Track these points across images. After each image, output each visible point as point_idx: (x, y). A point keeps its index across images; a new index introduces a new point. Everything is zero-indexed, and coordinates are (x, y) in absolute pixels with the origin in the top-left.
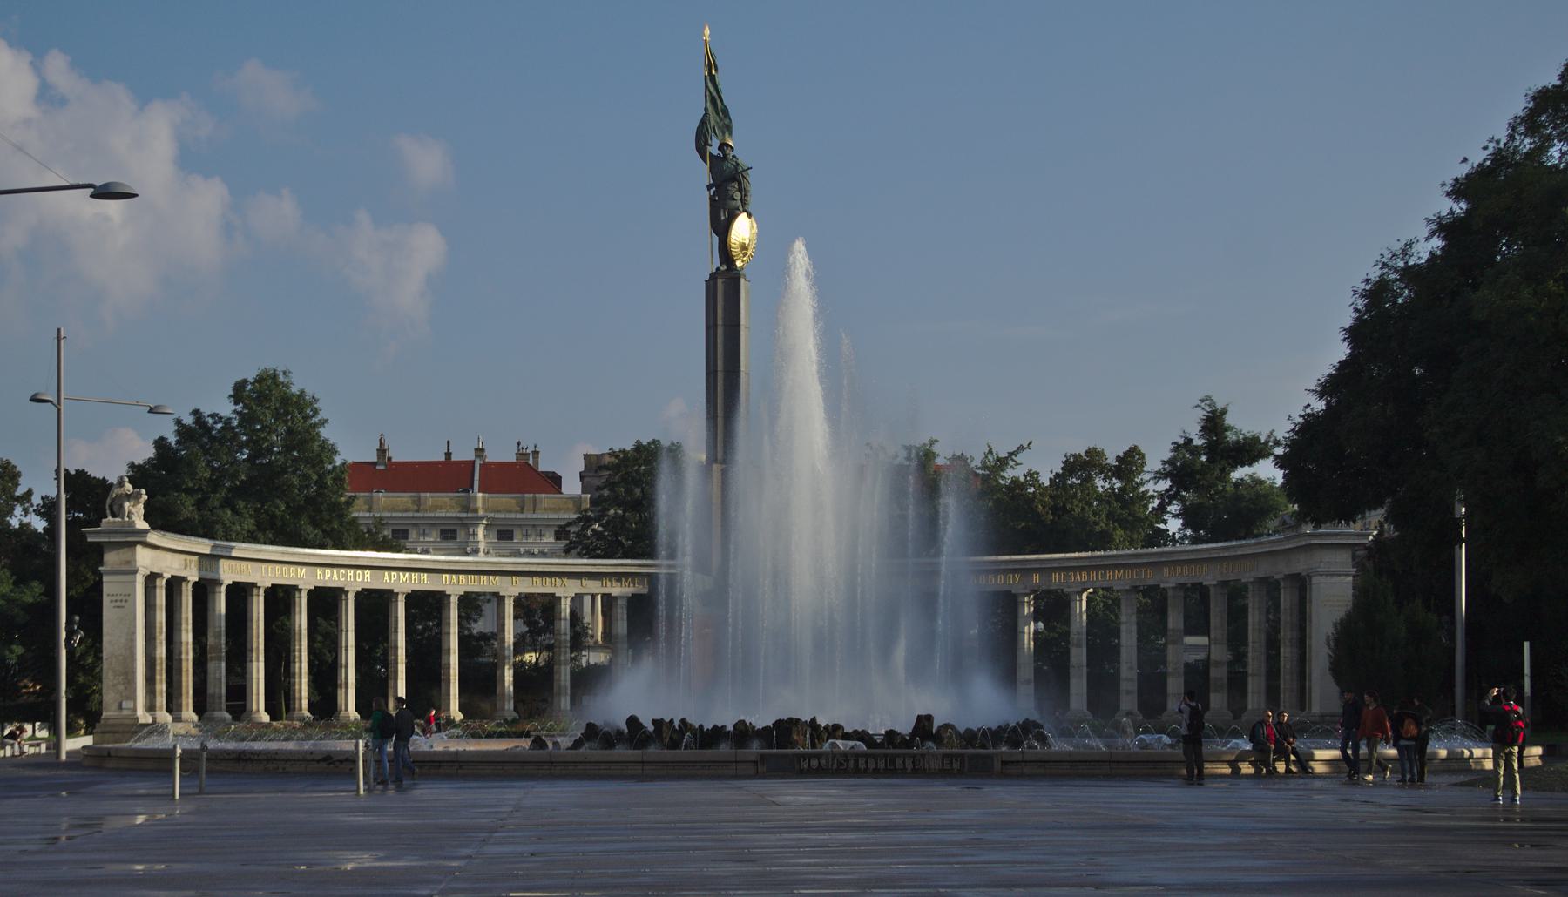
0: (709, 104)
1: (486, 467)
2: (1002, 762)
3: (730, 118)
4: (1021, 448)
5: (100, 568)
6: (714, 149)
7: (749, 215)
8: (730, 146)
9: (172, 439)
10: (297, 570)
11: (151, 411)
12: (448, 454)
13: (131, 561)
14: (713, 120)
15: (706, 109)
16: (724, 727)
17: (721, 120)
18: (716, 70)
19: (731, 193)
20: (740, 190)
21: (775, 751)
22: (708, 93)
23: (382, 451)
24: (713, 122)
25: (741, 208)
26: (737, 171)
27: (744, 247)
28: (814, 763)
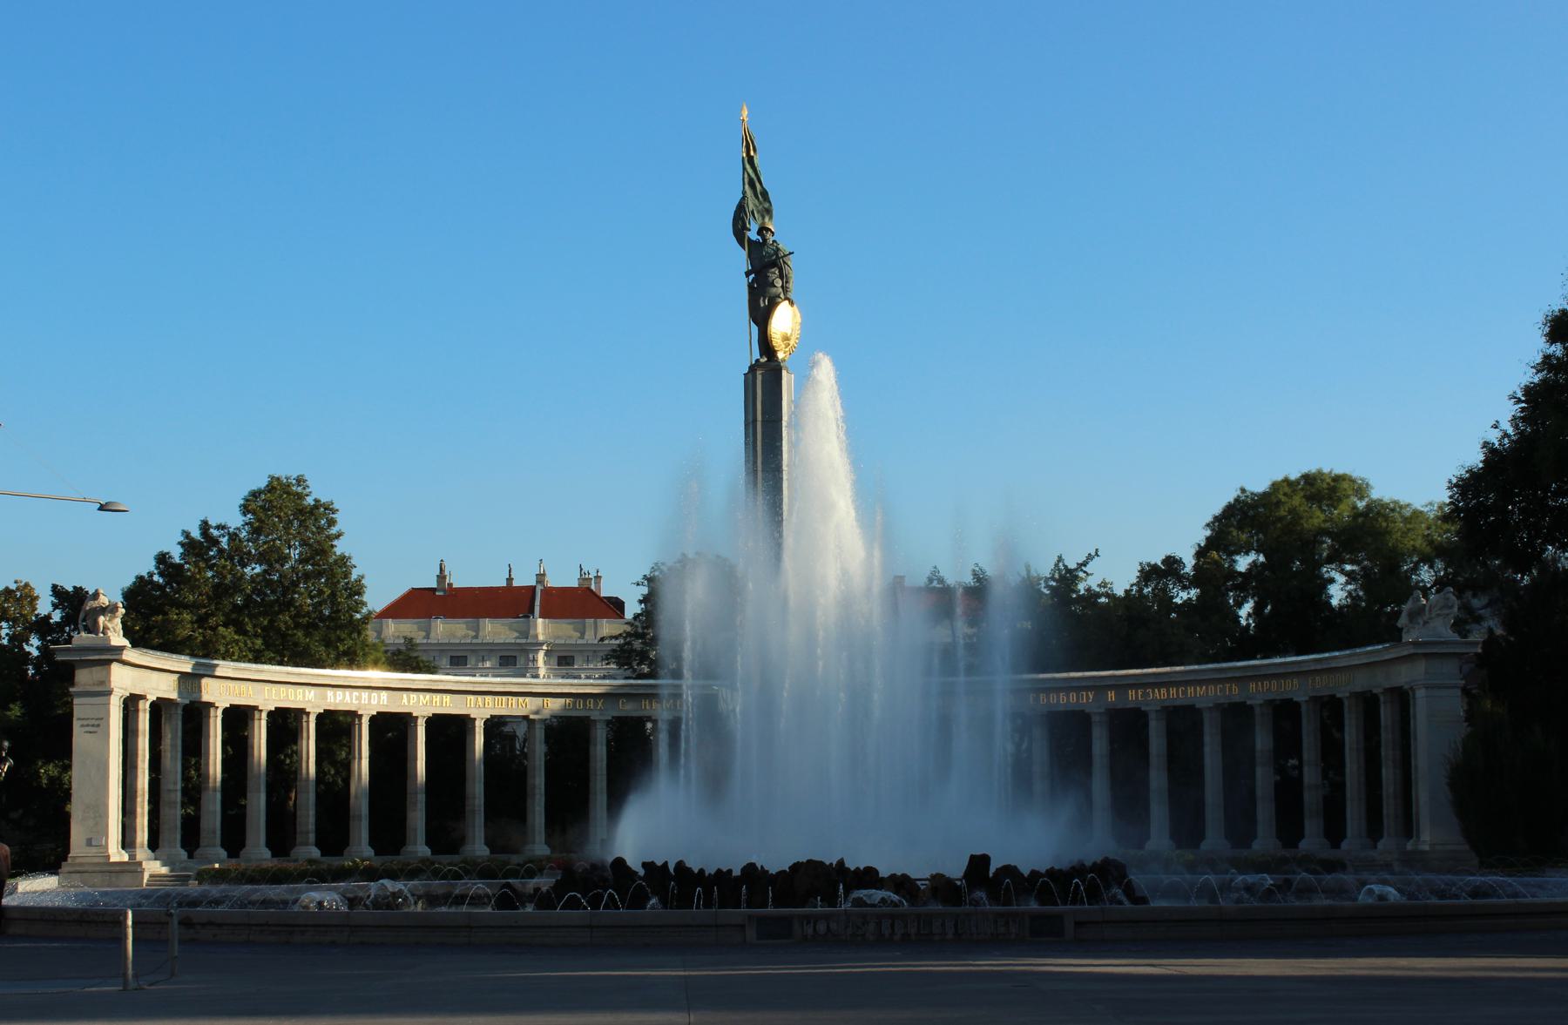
0: (747, 186)
1: (548, 592)
2: (1076, 923)
3: (770, 202)
4: (1090, 557)
5: (71, 690)
7: (792, 303)
8: (770, 230)
9: (176, 553)
10: (304, 693)
11: (102, 508)
12: (510, 580)
13: (106, 680)
14: (751, 204)
15: (744, 192)
16: (730, 871)
17: (760, 203)
18: (755, 150)
19: (770, 279)
20: (781, 277)
21: (770, 910)
22: (746, 176)
23: (441, 577)
24: (751, 207)
25: (782, 296)
26: (777, 255)
27: (786, 338)
28: (822, 927)
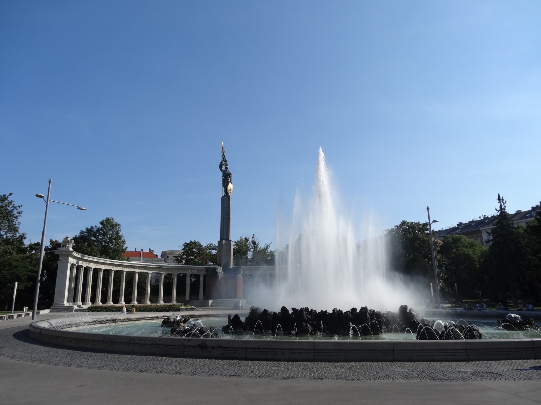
1: (143, 253)
6: (224, 168)
7: (232, 183)
11: (79, 208)
12: (135, 250)
14: (223, 162)
15: (222, 160)
24: (223, 163)
